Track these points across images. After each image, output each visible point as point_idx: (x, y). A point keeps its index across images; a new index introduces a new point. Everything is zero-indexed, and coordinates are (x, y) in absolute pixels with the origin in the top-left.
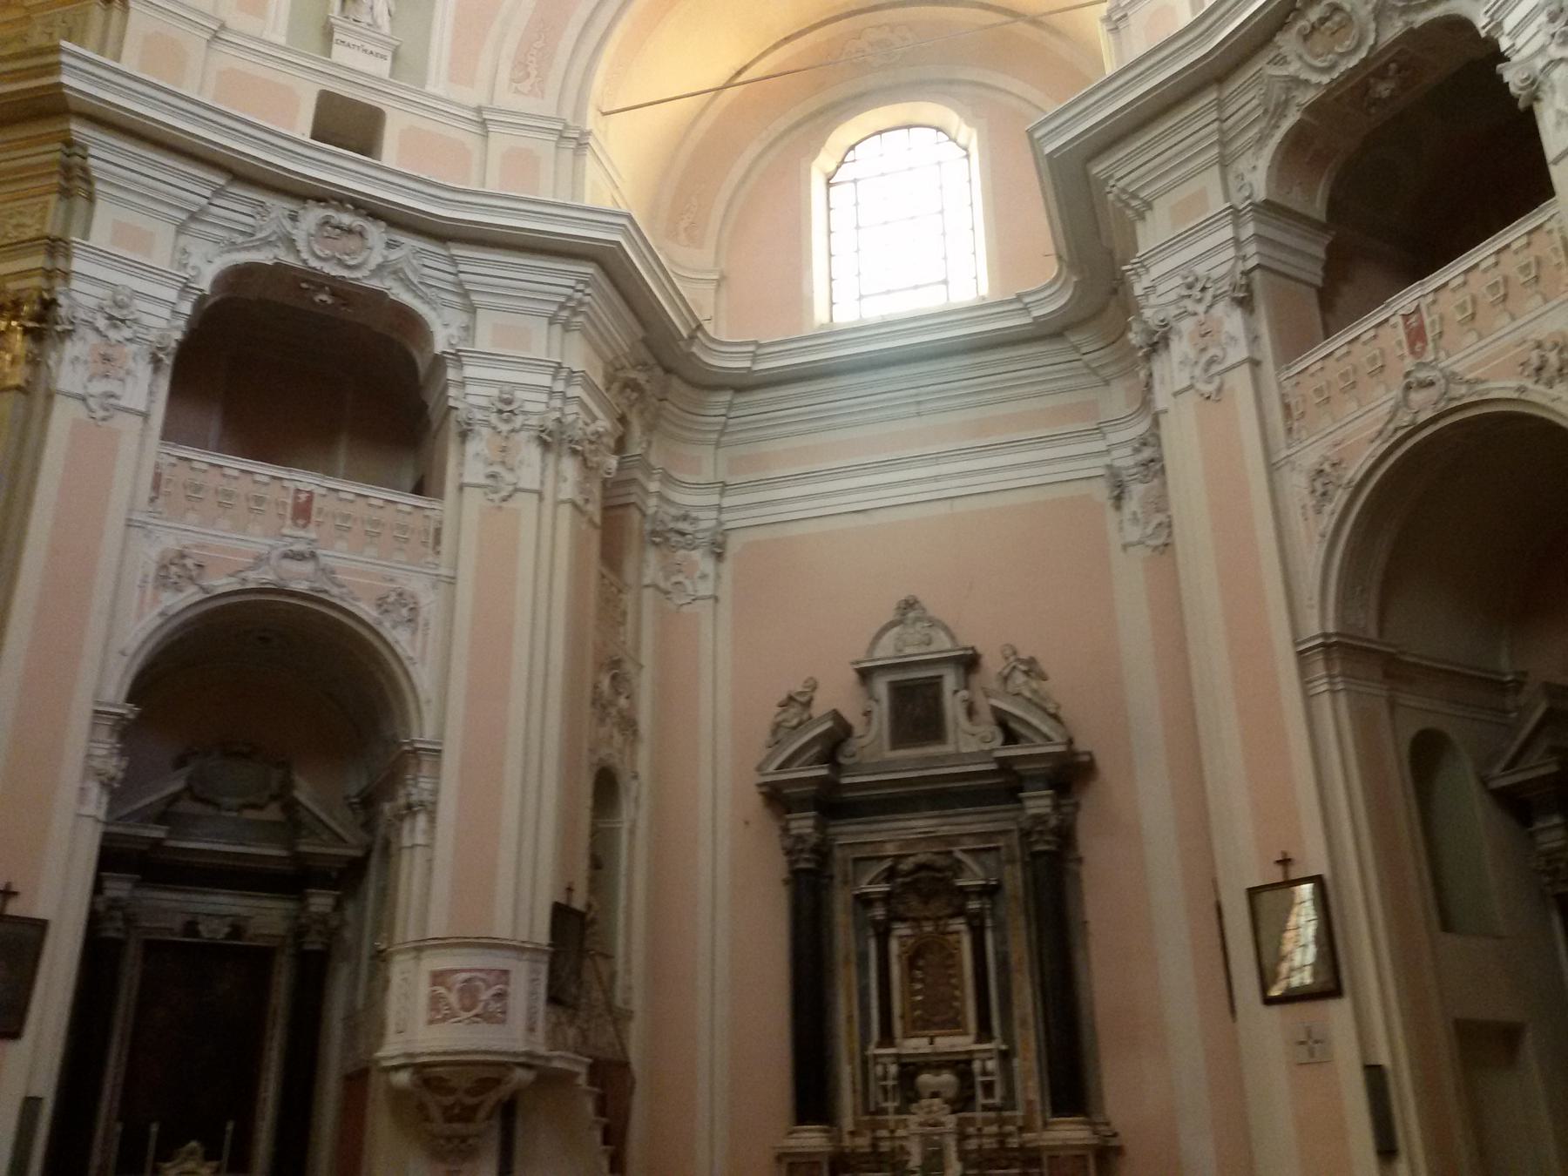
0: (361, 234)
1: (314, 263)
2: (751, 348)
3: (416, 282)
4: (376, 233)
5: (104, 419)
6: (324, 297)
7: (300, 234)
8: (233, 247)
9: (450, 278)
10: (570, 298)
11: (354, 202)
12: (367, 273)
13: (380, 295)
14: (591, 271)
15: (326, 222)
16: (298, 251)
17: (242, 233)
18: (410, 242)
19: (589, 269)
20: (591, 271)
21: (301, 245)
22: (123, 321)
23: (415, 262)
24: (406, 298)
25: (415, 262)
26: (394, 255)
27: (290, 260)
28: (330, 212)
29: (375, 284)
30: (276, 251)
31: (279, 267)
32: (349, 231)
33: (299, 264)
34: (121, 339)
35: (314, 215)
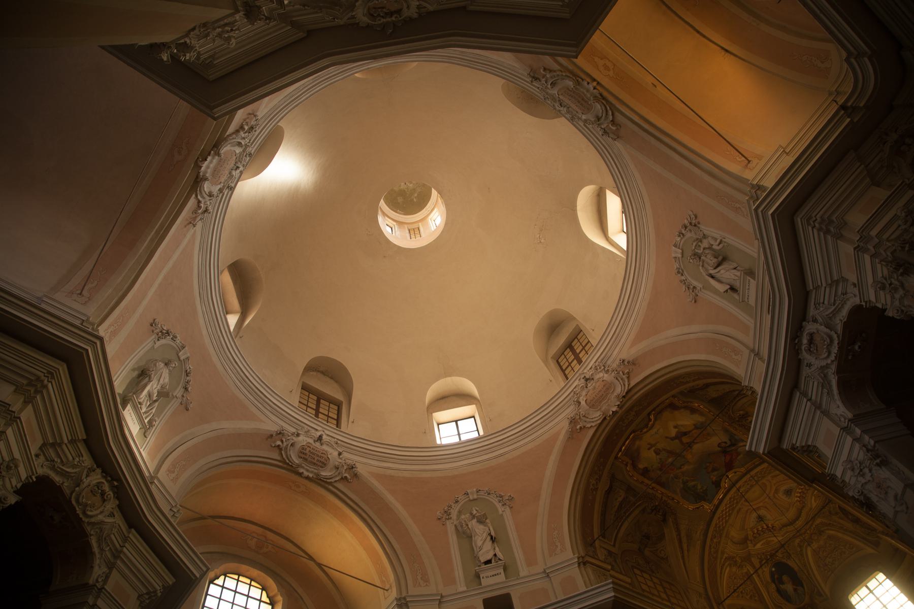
0: (811, 335)
1: (833, 357)
2: (853, 60)
3: (833, 308)
4: (810, 327)
5: (907, 508)
6: (856, 347)
7: (817, 363)
8: (830, 393)
9: (828, 290)
10: (819, 230)
11: (793, 339)
12: (833, 333)
13: (846, 325)
14: (799, 220)
15: (809, 351)
16: (827, 364)
17: (822, 386)
18: (812, 311)
19: (798, 221)
20: (799, 220)
21: (824, 363)
22: (861, 470)
23: (821, 309)
24: (845, 312)
25: (821, 309)
26: (820, 320)
27: (834, 367)
28: (803, 348)
29: (839, 328)
30: (830, 373)
31: (838, 372)
32: (811, 341)
33: (835, 363)
34: (870, 474)
35: (806, 356)
